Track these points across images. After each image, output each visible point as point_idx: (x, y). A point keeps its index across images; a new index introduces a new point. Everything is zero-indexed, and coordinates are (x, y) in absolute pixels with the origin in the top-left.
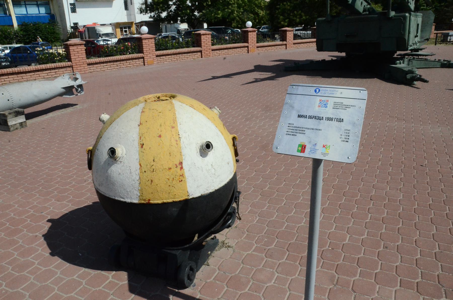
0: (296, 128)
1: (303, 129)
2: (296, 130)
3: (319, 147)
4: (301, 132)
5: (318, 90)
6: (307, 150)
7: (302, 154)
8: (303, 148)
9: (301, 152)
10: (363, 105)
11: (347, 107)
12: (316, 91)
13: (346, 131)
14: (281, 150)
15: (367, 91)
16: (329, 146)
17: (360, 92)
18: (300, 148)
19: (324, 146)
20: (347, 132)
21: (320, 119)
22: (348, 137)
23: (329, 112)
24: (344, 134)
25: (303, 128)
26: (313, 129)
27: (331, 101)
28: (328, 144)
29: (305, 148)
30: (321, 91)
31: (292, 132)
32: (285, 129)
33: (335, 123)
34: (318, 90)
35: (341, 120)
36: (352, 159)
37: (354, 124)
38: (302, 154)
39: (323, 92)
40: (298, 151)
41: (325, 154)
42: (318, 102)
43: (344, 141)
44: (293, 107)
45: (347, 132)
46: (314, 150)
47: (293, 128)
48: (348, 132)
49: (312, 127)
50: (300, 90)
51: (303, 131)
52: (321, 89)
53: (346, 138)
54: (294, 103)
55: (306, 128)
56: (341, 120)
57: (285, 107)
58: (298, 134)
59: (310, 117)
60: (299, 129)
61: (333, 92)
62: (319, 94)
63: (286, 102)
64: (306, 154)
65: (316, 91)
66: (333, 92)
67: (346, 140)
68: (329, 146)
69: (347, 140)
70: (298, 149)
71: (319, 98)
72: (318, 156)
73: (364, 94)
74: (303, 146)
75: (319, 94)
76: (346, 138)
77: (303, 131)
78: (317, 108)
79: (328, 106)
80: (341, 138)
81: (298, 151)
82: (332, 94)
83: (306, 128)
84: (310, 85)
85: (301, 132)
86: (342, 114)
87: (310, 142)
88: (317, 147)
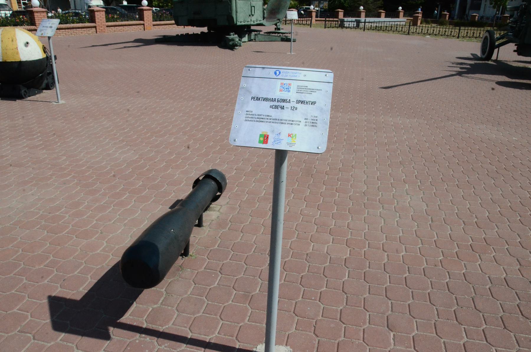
5: (278, 72)
6: (270, 140)
7: (264, 146)
8: (265, 139)
9: (264, 143)
10: (329, 88)
11: (312, 91)
12: (275, 73)
17: (326, 75)
18: (262, 139)
19: (289, 135)
27: (294, 85)
28: (294, 132)
29: (267, 138)
32: (243, 118)
38: (264, 146)
39: (284, 74)
40: (260, 142)
42: (279, 85)
46: (279, 141)
50: (258, 72)
57: (240, 92)
61: (296, 75)
63: (241, 86)
64: (269, 145)
65: (275, 73)
66: (296, 75)
68: (295, 135)
71: (279, 82)
72: (282, 147)
73: (330, 76)
74: (265, 136)
79: (291, 90)
81: (260, 142)
87: (273, 131)
88: (281, 137)
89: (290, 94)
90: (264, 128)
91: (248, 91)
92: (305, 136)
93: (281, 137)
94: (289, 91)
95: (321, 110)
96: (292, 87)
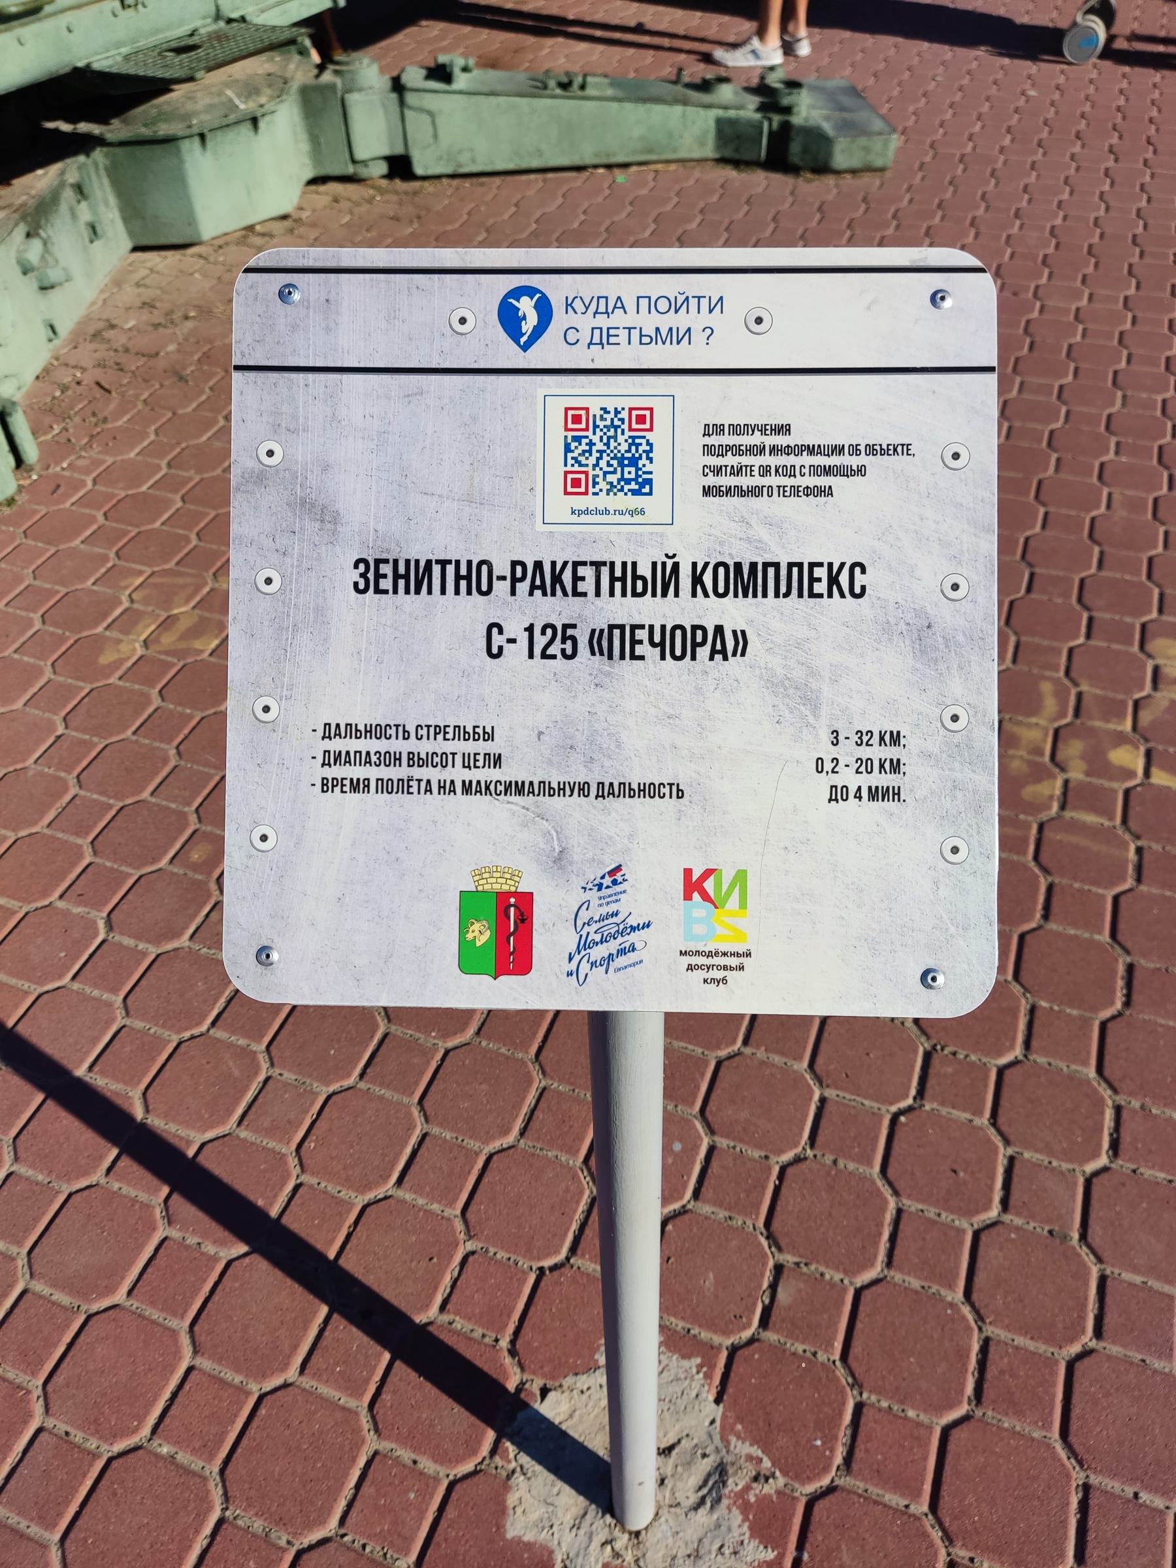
3: (650, 893)
5: (526, 306)
6: (551, 939)
8: (510, 930)
9: (501, 970)
12: (509, 318)
18: (482, 934)
30: (560, 321)
34: (526, 306)
39: (585, 323)
40: (467, 962)
46: (609, 938)
52: (556, 289)
54: (326, 468)
57: (248, 520)
61: (680, 321)
63: (241, 460)
64: (544, 989)
66: (680, 321)
68: (741, 877)
70: (465, 946)
73: (971, 317)
75: (546, 352)
78: (560, 505)
79: (659, 469)
81: (467, 962)
87: (559, 860)
88: (634, 904)
89: (655, 505)
90: (485, 840)
93: (634, 904)
94: (644, 486)
95: (923, 635)
96: (659, 437)
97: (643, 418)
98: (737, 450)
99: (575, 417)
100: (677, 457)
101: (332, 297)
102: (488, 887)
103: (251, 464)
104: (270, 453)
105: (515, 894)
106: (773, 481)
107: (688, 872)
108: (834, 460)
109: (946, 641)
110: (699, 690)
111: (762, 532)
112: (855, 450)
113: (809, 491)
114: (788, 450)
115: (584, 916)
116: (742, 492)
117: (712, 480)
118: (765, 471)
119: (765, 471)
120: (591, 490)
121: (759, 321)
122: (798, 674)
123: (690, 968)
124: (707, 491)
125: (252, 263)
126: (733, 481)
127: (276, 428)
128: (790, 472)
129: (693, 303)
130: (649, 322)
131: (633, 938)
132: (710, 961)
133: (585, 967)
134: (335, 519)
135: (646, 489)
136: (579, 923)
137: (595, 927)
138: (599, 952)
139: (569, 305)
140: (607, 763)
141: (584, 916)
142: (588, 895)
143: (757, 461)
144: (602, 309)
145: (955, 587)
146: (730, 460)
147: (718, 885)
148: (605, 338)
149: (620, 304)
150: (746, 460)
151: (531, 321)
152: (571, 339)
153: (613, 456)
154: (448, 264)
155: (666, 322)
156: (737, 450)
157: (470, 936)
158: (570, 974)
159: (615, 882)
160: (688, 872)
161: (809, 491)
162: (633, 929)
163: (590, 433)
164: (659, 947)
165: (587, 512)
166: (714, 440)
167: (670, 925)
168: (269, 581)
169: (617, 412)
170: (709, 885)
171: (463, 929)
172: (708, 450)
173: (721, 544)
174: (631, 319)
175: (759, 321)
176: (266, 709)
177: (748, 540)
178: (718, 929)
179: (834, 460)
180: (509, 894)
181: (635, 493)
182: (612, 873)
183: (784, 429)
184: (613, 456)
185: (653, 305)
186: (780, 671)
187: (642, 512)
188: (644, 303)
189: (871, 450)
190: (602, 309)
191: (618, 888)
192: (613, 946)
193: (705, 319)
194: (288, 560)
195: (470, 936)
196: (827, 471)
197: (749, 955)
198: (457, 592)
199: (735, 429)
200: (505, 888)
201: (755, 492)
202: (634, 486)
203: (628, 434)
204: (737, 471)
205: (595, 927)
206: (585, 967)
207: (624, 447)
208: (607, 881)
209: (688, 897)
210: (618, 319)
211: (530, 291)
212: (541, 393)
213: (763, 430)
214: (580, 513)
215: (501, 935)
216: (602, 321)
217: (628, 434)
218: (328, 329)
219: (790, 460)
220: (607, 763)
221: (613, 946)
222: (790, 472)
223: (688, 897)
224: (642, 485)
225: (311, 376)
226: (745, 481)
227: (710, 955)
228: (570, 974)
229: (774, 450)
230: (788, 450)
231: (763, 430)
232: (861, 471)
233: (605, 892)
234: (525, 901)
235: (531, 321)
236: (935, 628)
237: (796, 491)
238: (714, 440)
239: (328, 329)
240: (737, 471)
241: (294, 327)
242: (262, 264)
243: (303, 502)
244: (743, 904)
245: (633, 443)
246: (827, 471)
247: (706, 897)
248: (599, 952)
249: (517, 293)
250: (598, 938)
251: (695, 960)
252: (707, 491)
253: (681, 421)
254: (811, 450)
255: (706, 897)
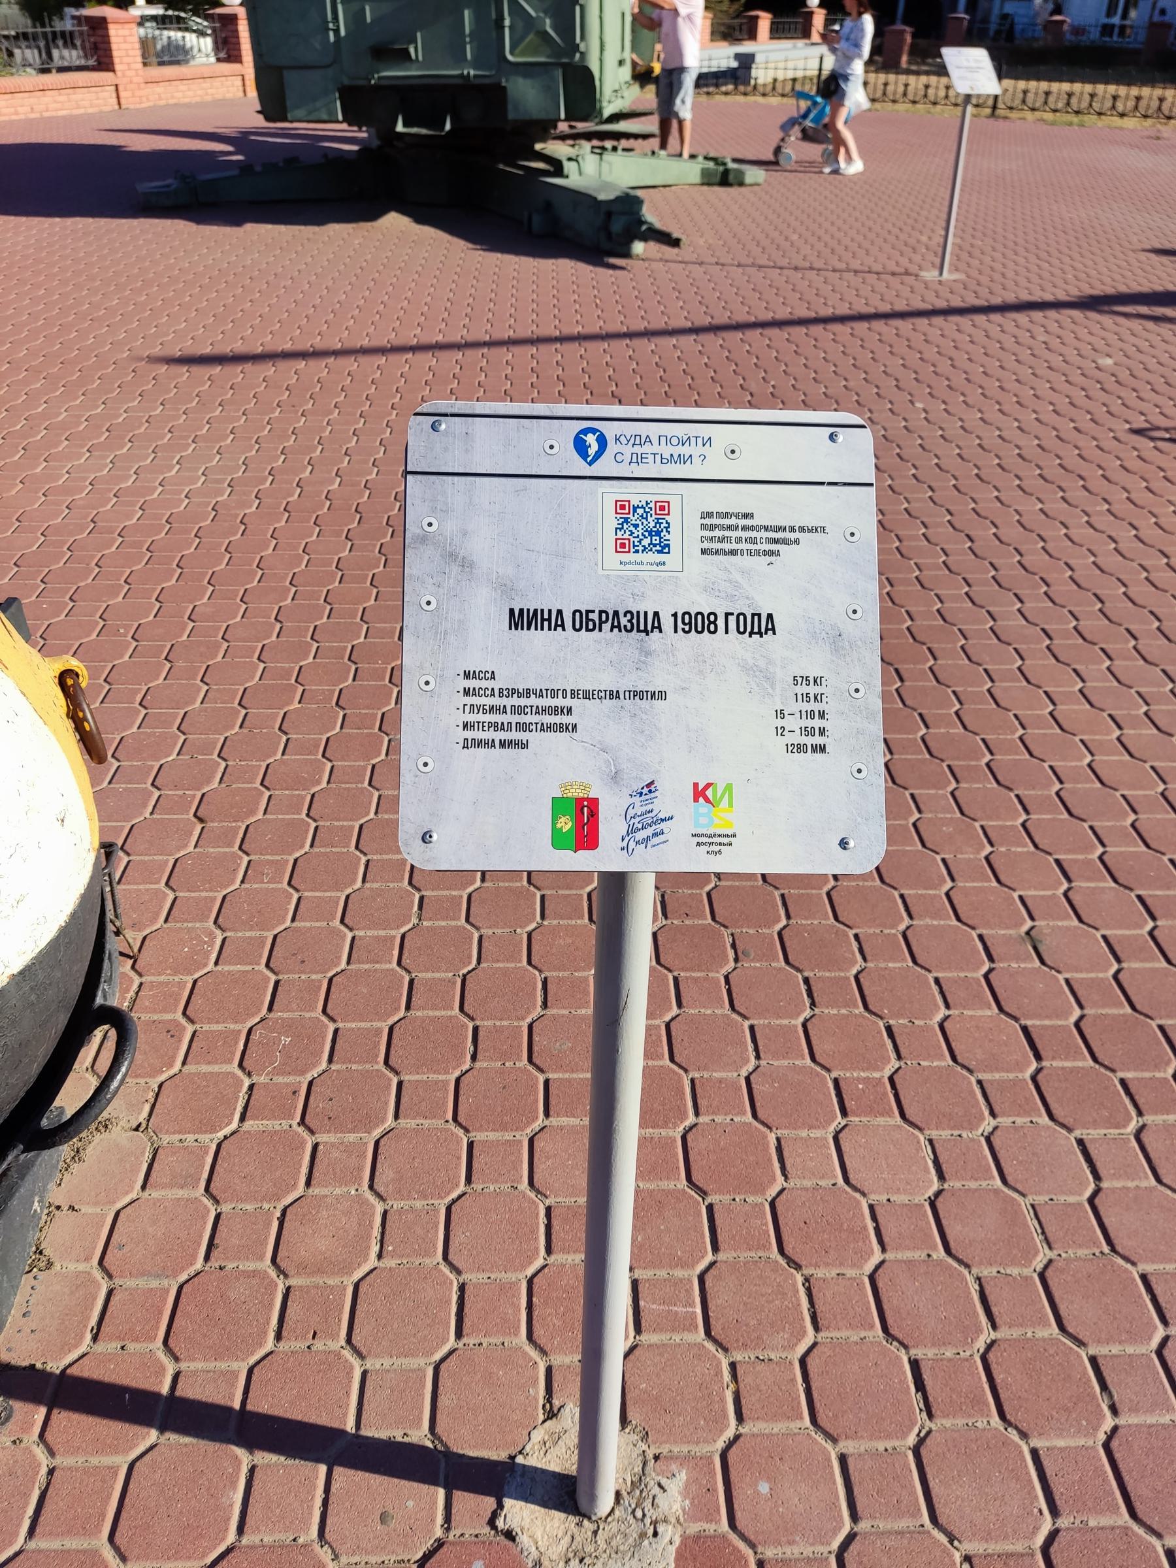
0: (515, 701)
1: (559, 702)
2: (519, 710)
3: (672, 798)
4: (548, 719)
5: (591, 439)
6: (611, 827)
7: (584, 861)
11: (779, 538)
12: (580, 446)
13: (802, 689)
14: (452, 850)
15: (867, 434)
16: (729, 787)
18: (567, 824)
19: (699, 793)
20: (809, 686)
21: (643, 624)
22: (817, 723)
23: (683, 578)
24: (793, 707)
25: (554, 693)
26: (614, 695)
28: (719, 776)
30: (612, 448)
31: (495, 726)
33: (727, 645)
35: (760, 625)
36: (867, 853)
37: (836, 640)
38: (584, 861)
39: (628, 450)
41: (713, 842)
42: (612, 522)
43: (801, 748)
44: (467, 565)
45: (809, 686)
46: (647, 827)
47: (496, 701)
48: (813, 690)
49: (607, 682)
50: (487, 444)
51: (557, 711)
53: (809, 732)
54: (465, 534)
55: (574, 694)
56: (760, 625)
58: (532, 737)
59: (585, 621)
60: (533, 701)
61: (685, 450)
62: (604, 466)
63: (412, 530)
66: (685, 450)
67: (809, 741)
68: (729, 787)
69: (818, 740)
74: (579, 802)
76: (809, 732)
77: (557, 711)
78: (613, 559)
79: (673, 538)
80: (781, 731)
81: (557, 841)
82: (682, 459)
83: (574, 694)
84: (541, 408)
85: (548, 719)
86: (760, 584)
87: (615, 778)
88: (662, 805)
89: (671, 560)
91: (453, 556)
92: (766, 777)
93: (662, 805)
94: (664, 548)
97: (664, 507)
98: (722, 527)
99: (621, 506)
100: (685, 531)
101: (470, 431)
102: (570, 795)
103: (418, 531)
104: (430, 525)
105: (588, 799)
106: (743, 546)
107: (696, 785)
108: (780, 535)
109: (851, 644)
110: (701, 672)
111: (737, 576)
112: (792, 529)
113: (765, 553)
114: (752, 528)
115: (631, 812)
116: (725, 553)
117: (706, 545)
118: (739, 540)
119: (739, 540)
120: (632, 550)
121: (733, 452)
122: (762, 663)
123: (698, 844)
124: (704, 552)
125: (418, 410)
126: (719, 546)
127: (434, 510)
128: (754, 541)
129: (693, 440)
130: (667, 451)
131: (662, 826)
132: (710, 840)
133: (632, 844)
134: (472, 565)
135: (666, 550)
136: (628, 817)
137: (638, 819)
138: (641, 835)
139: (617, 439)
140: (644, 717)
141: (631, 812)
142: (634, 799)
143: (734, 534)
144: (638, 442)
145: (855, 612)
146: (717, 533)
147: (715, 792)
148: (640, 459)
149: (648, 440)
150: (727, 533)
151: (594, 448)
152: (619, 458)
153: (645, 531)
154: (542, 414)
155: (676, 451)
156: (722, 527)
157: (559, 826)
158: (623, 849)
159: (650, 791)
160: (696, 785)
161: (765, 553)
162: (662, 820)
163: (631, 516)
164: (678, 832)
165: (630, 563)
166: (707, 521)
167: (687, 819)
168: (429, 603)
169: (647, 503)
170: (709, 793)
171: (554, 821)
172: (704, 527)
173: (713, 583)
174: (655, 448)
175: (733, 452)
176: (427, 683)
177: (730, 581)
178: (719, 819)
179: (780, 535)
180: (583, 799)
181: (659, 552)
182: (648, 785)
183: (750, 516)
184: (645, 531)
185: (668, 441)
186: (751, 662)
187: (664, 563)
188: (663, 439)
189: (802, 529)
190: (638, 442)
191: (653, 795)
192: (649, 831)
193: (700, 449)
194: (441, 590)
195: (559, 826)
196: (776, 541)
197: (735, 836)
198: (550, 611)
199: (720, 515)
200: (581, 795)
201: (733, 552)
202: (658, 548)
203: (654, 516)
204: (722, 540)
205: (638, 819)
206: (632, 844)
207: (652, 524)
208: (646, 790)
209: (696, 800)
210: (647, 448)
211: (594, 431)
212: (600, 491)
213: (737, 516)
214: (626, 564)
215: (579, 824)
216: (637, 449)
217: (654, 516)
218: (467, 451)
219: (754, 534)
220: (644, 717)
221: (649, 831)
222: (754, 541)
223: (696, 800)
224: (663, 548)
225: (456, 478)
226: (727, 546)
227: (710, 836)
228: (623, 849)
229: (744, 528)
230: (752, 528)
231: (737, 516)
232: (797, 541)
233: (644, 797)
234: (594, 803)
235: (594, 448)
236: (844, 636)
237: (757, 552)
238: (707, 521)
239: (467, 451)
240: (722, 540)
241: (446, 449)
242: (425, 411)
243: (451, 555)
244: (731, 805)
245: (658, 522)
246: (776, 541)
247: (707, 800)
248: (641, 835)
249: (586, 431)
250: (640, 826)
251: (701, 840)
252: (704, 552)
253: (687, 509)
254: (766, 529)
255: (707, 800)
